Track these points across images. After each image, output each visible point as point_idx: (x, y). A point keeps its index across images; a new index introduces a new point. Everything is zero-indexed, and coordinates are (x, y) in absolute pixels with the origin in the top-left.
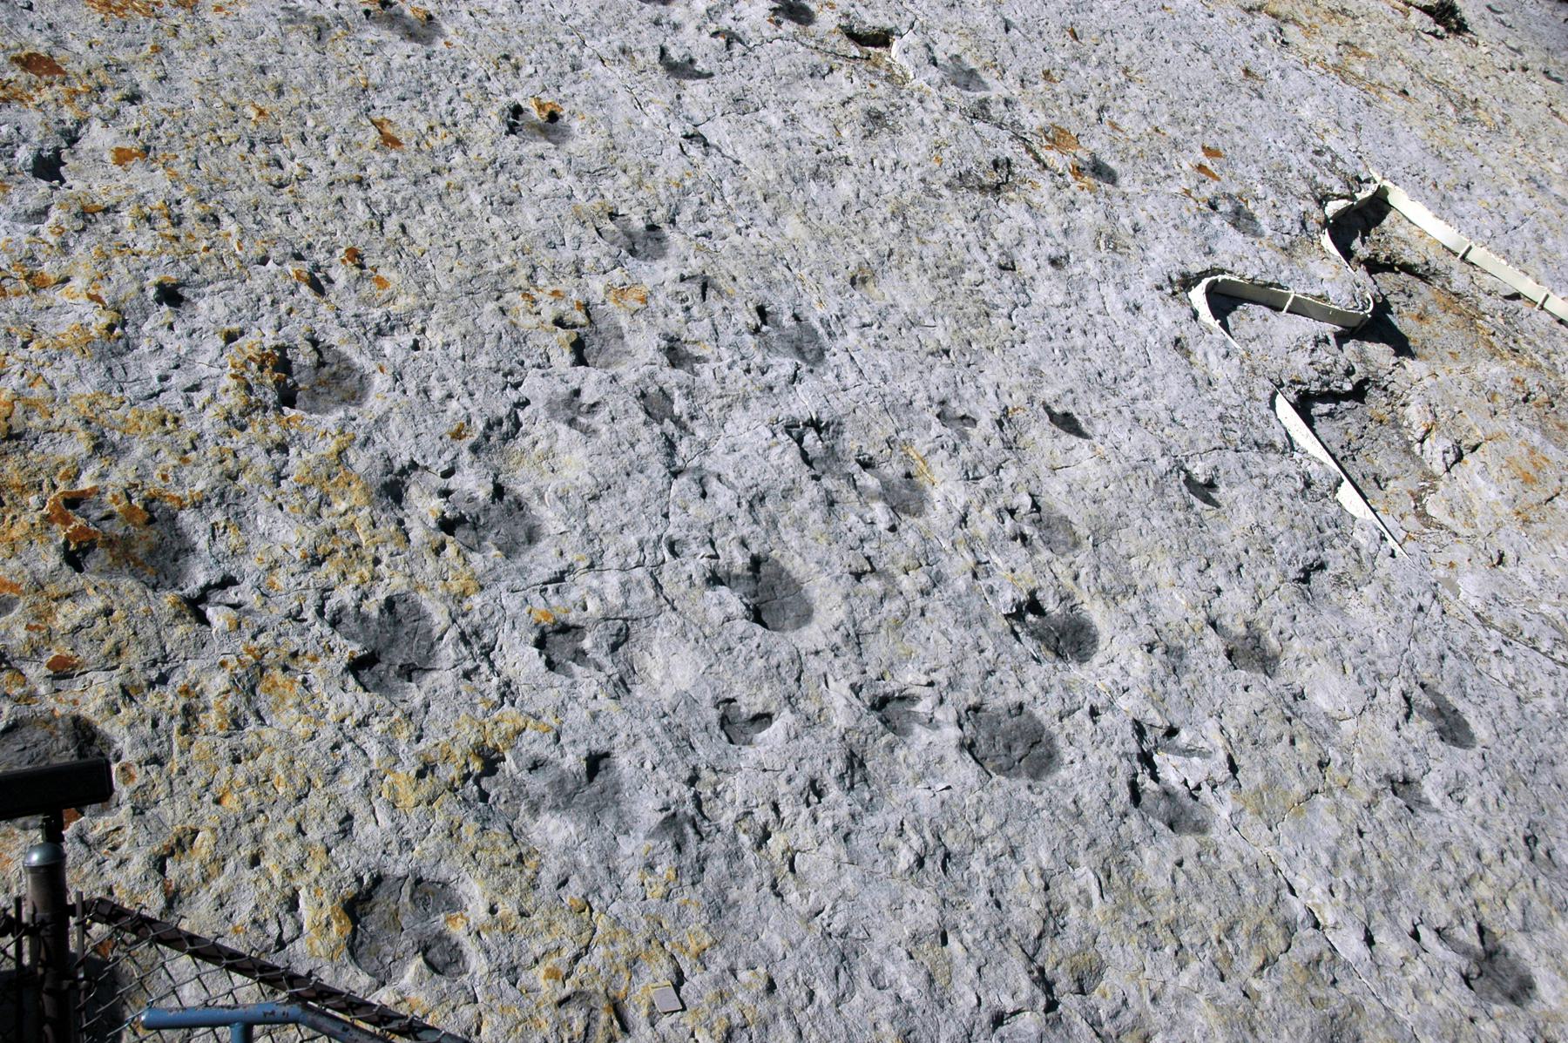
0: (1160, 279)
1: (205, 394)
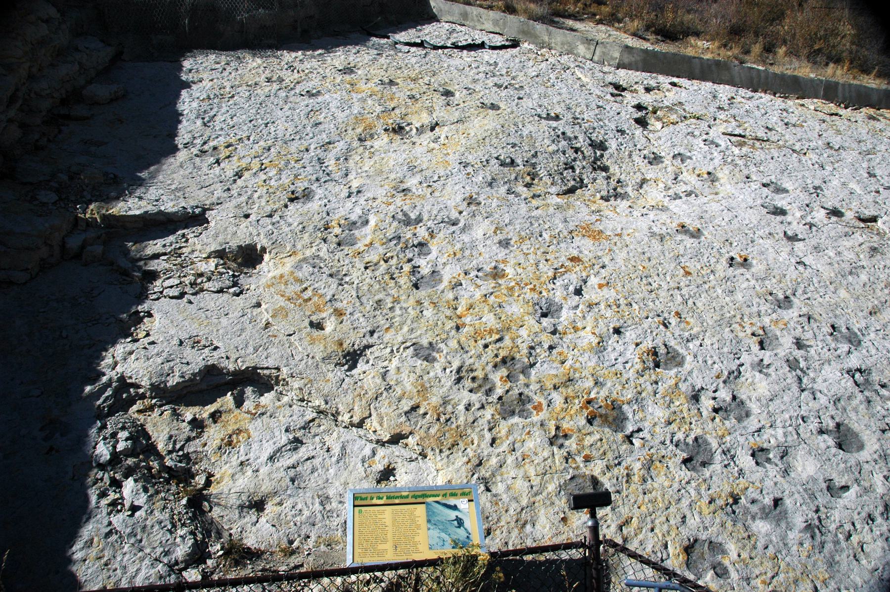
1: (630, 365)
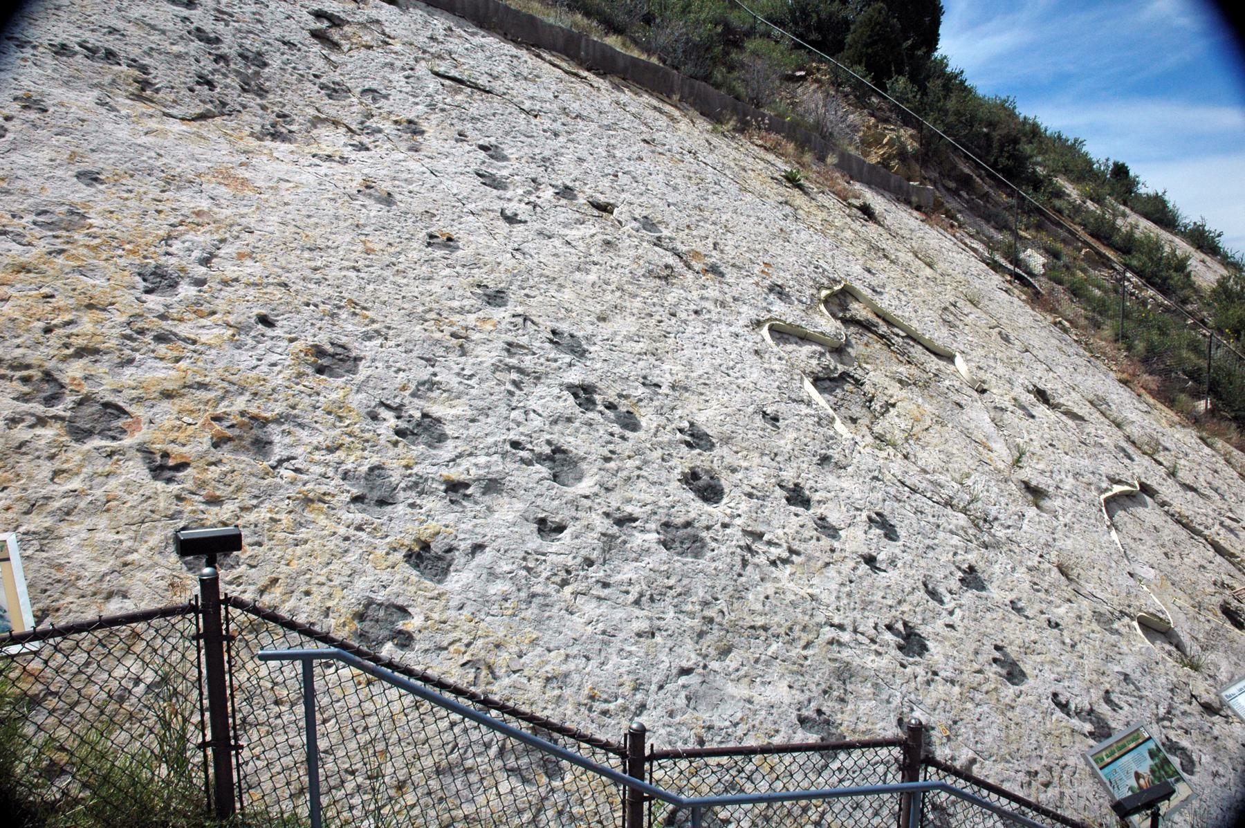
0: (747, 322)
1: (279, 368)
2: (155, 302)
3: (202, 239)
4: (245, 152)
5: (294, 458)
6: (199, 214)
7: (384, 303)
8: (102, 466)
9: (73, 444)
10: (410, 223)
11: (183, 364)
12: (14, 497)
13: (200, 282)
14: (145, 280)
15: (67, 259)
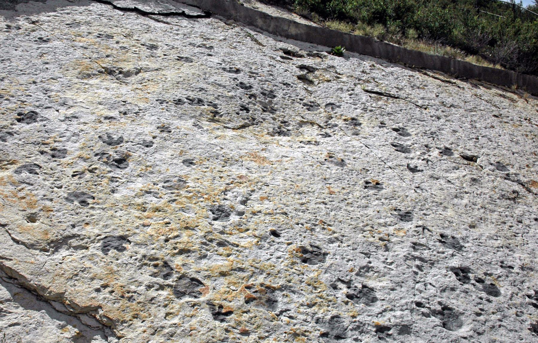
1: (282, 259)
2: (218, 224)
3: (242, 191)
4: (264, 143)
5: (289, 310)
6: (241, 177)
7: (340, 222)
8: (189, 311)
9: (176, 299)
10: (354, 175)
11: (231, 258)
12: (147, 326)
13: (241, 214)
14: (213, 213)
15: (177, 204)
